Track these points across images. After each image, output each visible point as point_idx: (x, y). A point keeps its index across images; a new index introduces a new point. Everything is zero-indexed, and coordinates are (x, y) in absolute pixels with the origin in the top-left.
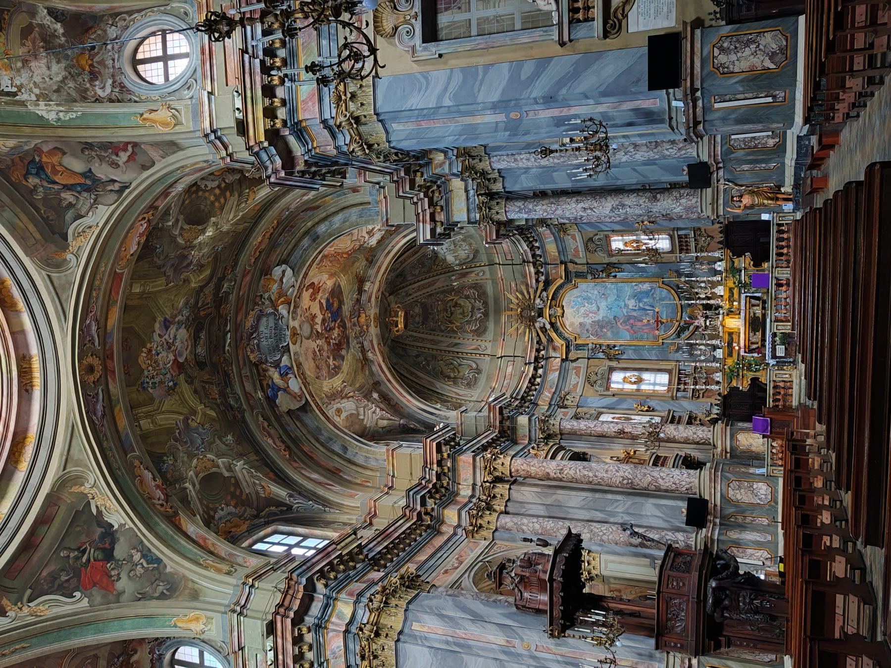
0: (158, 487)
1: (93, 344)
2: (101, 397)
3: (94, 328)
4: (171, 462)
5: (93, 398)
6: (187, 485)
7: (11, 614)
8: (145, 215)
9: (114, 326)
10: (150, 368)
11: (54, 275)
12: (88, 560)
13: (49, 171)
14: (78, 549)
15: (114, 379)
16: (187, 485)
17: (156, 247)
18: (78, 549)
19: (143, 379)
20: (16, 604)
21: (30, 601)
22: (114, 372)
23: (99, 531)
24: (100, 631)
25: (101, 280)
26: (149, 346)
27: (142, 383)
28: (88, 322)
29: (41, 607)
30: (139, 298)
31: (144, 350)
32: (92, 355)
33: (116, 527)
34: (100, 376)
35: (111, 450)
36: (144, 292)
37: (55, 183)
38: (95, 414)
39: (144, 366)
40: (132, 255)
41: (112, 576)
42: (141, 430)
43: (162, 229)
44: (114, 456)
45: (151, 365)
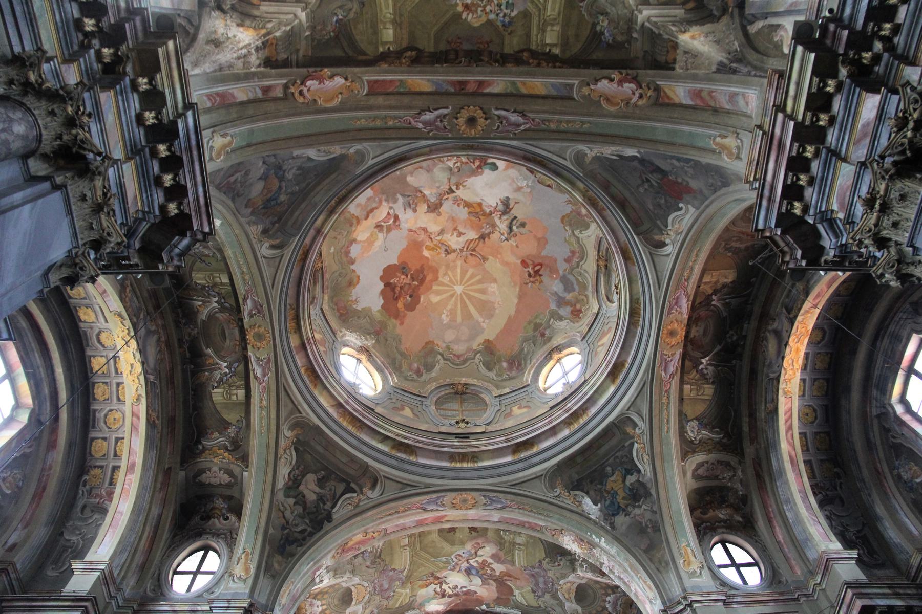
0: (621, 83)
1: (445, 116)
2: (503, 113)
3: (428, 116)
4: (606, 23)
5: (502, 123)
6: (640, 18)
7: (667, 241)
8: (297, 95)
9: (428, 80)
10: (488, 8)
11: (372, 156)
12: (657, 182)
13: (270, 195)
14: (643, 182)
15: (489, 84)
16: (640, 18)
17: (337, 21)
18: (643, 182)
19: (499, 24)
20: (663, 234)
21: (666, 226)
22: (481, 83)
23: (635, 163)
24: (724, 215)
25: (375, 118)
26: (460, 8)
27: (504, 25)
28: (420, 126)
29: (676, 226)
30: (401, 29)
31: (463, 17)
32: (457, 118)
33: (638, 155)
34: (481, 109)
35: (561, 122)
36: (394, 22)
37: (280, 188)
38: (519, 125)
39: (484, 19)
40: (346, 79)
41: (681, 183)
42: (555, 45)
43: (313, 28)
44: (568, 122)
45: (485, 6)
